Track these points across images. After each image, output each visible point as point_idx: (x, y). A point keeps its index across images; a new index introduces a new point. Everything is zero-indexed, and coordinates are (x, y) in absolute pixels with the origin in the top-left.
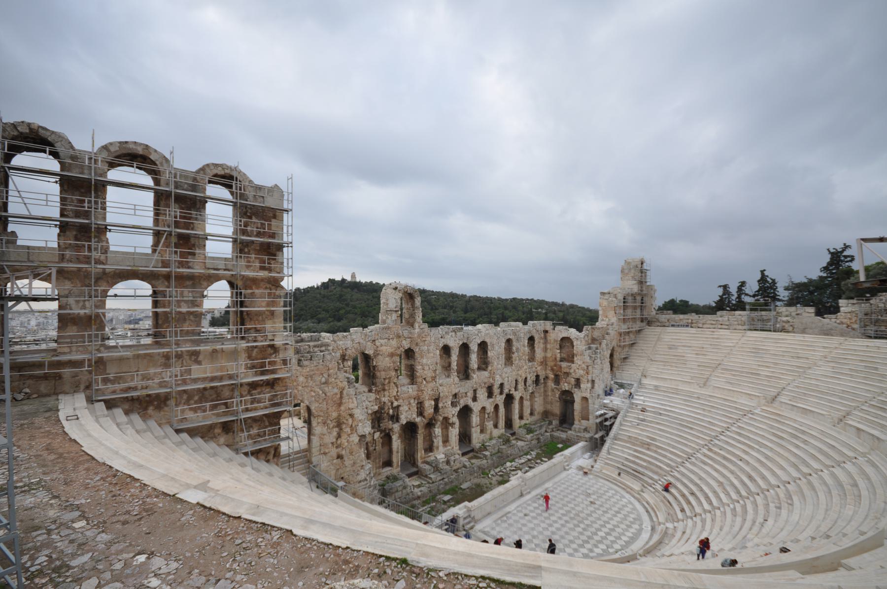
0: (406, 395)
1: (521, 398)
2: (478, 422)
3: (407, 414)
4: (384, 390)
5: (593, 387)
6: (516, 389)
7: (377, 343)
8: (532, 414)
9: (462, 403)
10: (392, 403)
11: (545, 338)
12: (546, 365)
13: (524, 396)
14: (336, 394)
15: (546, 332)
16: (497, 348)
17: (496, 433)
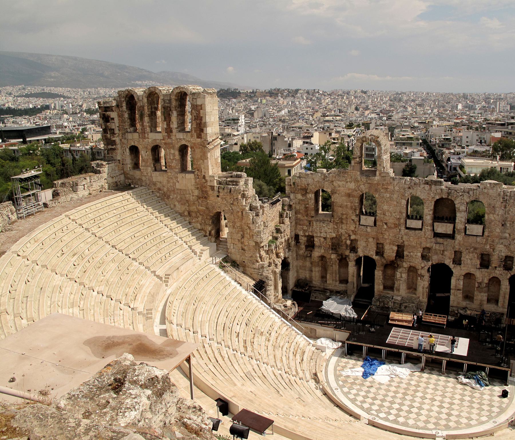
0: (363, 233)
2: (462, 286)
4: (342, 223)
9: (435, 259)
10: (350, 236)
14: (238, 212)
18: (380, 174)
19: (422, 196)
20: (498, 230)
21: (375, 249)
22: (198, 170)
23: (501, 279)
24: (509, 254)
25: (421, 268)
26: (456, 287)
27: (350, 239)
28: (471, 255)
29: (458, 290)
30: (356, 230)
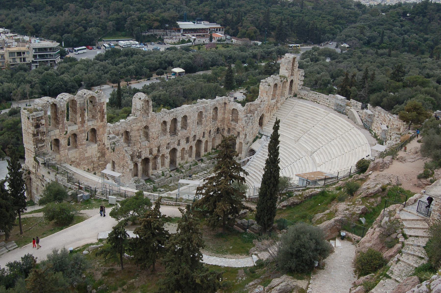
1: (207, 141)
3: (145, 154)
5: (245, 137)
6: (203, 137)
7: (132, 126)
8: (213, 149)
9: (172, 147)
11: (225, 107)
13: (209, 140)
15: (225, 103)
16: (192, 118)
17: (190, 160)
19: (167, 120)
22: (100, 141)
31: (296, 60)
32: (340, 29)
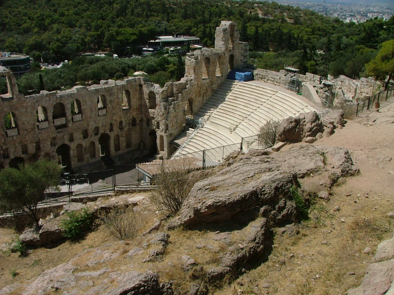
2: (76, 154)
6: (111, 130)
9: (59, 143)
12: (142, 110)
16: (89, 103)
18: (17, 97)
20: (89, 114)
21: (21, 150)
23: (95, 142)
24: (96, 125)
25: (52, 152)
26: (73, 155)
27: (3, 150)
28: (78, 133)
29: (75, 157)
30: (6, 141)
31: (236, 28)
32: (317, 39)
